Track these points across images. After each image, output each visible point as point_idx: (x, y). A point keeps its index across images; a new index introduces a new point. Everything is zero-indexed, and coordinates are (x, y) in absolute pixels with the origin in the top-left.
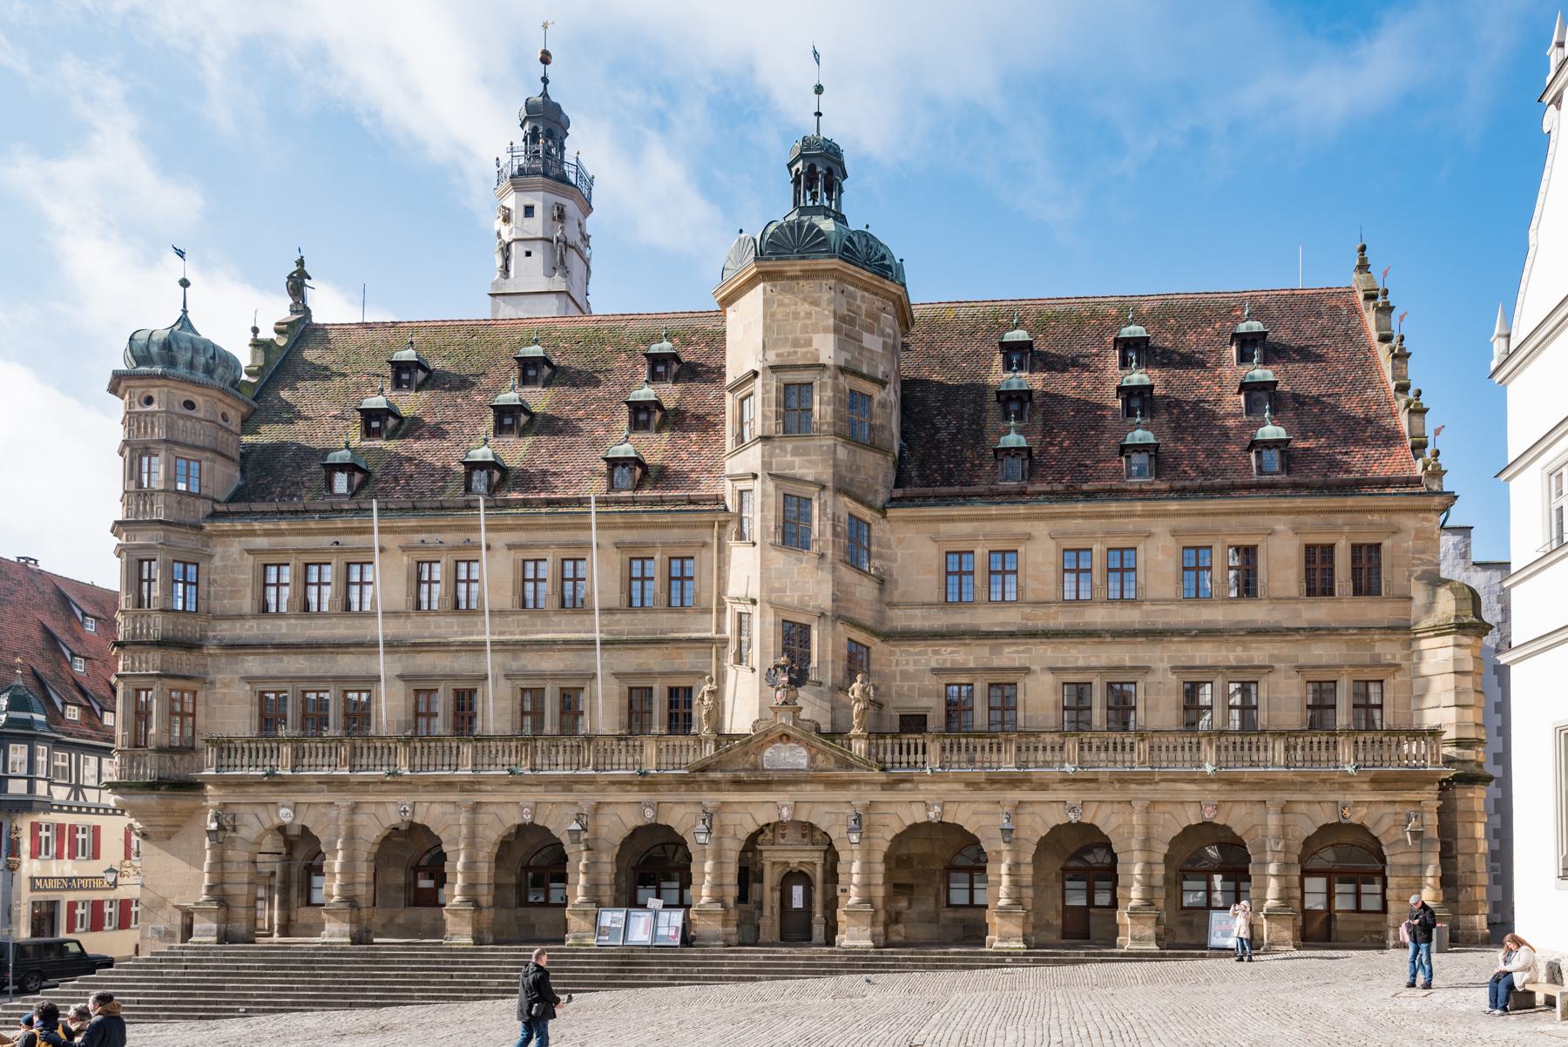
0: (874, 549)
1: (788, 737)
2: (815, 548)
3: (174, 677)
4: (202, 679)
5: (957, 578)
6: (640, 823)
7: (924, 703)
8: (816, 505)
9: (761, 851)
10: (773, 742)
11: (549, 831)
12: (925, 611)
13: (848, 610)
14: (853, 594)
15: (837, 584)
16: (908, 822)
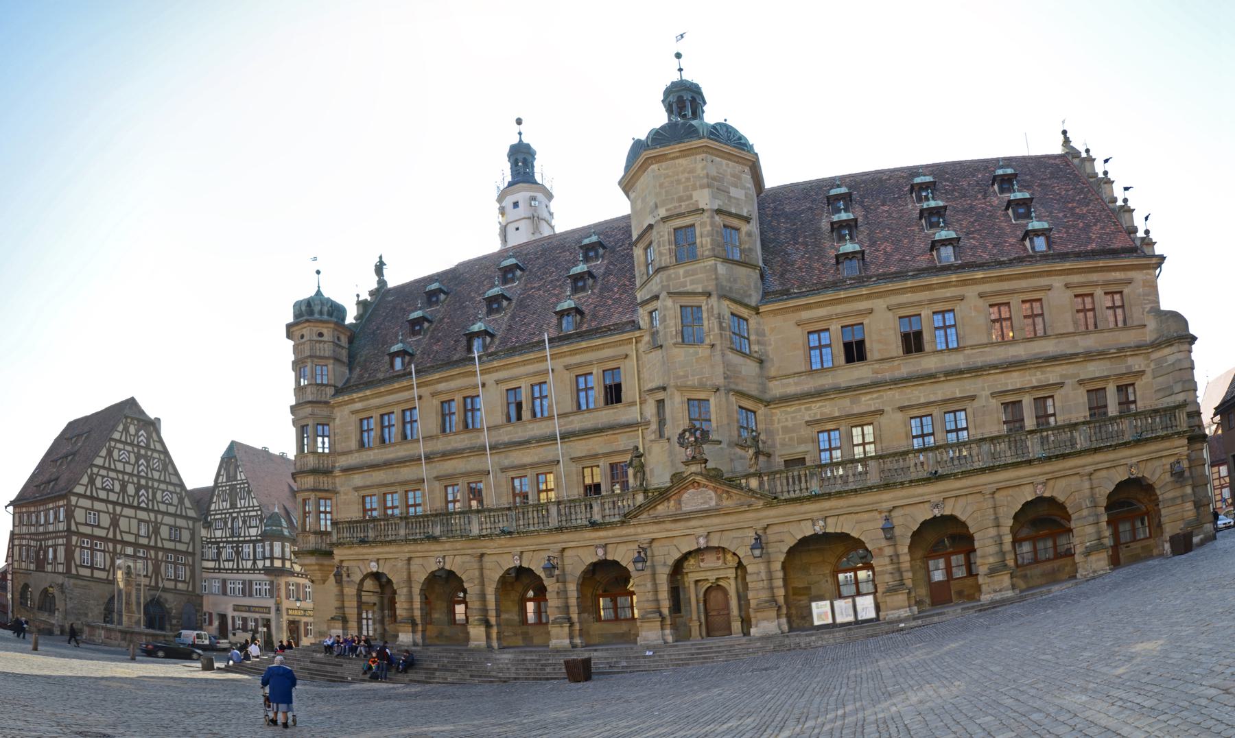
0: (752, 338)
1: (698, 483)
2: (707, 341)
3: (320, 490)
4: (334, 492)
5: (818, 351)
6: (595, 560)
7: (802, 448)
8: (704, 308)
9: (687, 573)
10: (686, 488)
11: (532, 571)
12: (796, 379)
13: (737, 384)
14: (740, 372)
15: (727, 365)
16: (799, 537)
